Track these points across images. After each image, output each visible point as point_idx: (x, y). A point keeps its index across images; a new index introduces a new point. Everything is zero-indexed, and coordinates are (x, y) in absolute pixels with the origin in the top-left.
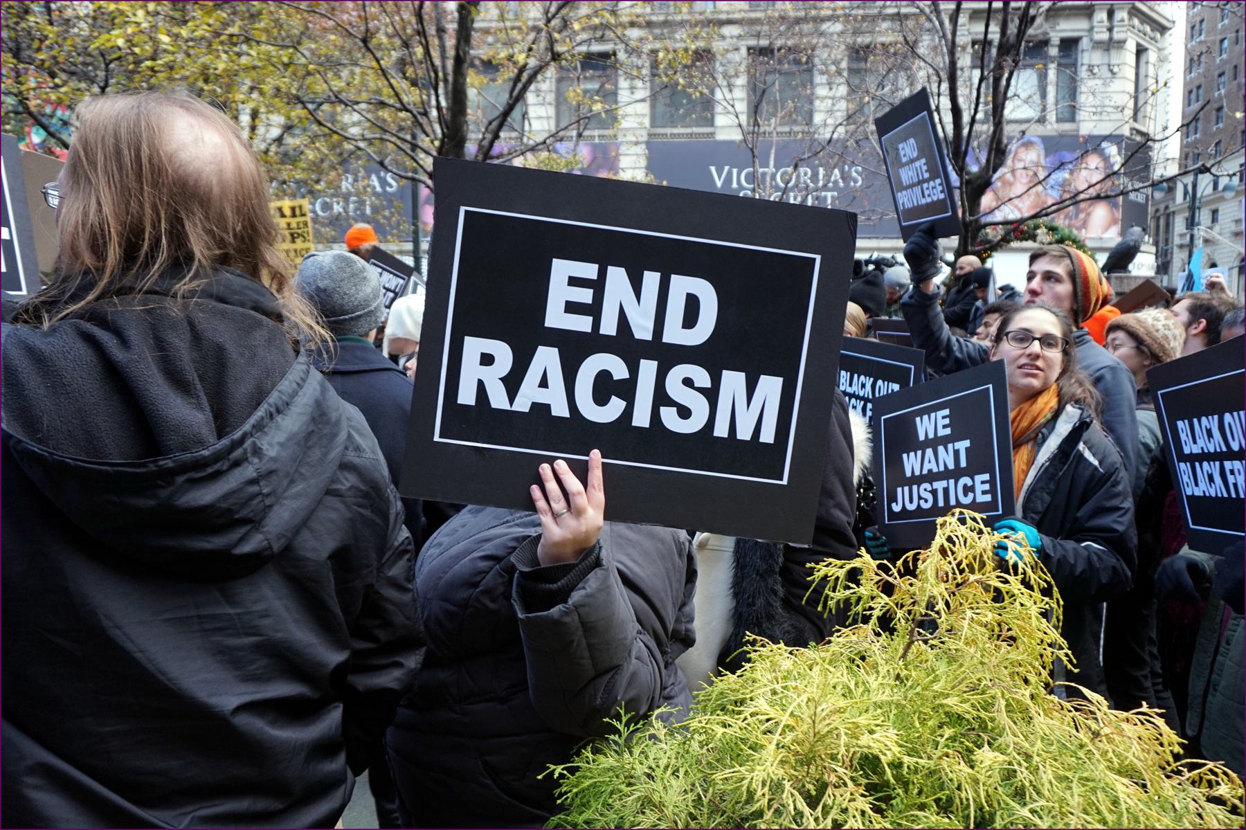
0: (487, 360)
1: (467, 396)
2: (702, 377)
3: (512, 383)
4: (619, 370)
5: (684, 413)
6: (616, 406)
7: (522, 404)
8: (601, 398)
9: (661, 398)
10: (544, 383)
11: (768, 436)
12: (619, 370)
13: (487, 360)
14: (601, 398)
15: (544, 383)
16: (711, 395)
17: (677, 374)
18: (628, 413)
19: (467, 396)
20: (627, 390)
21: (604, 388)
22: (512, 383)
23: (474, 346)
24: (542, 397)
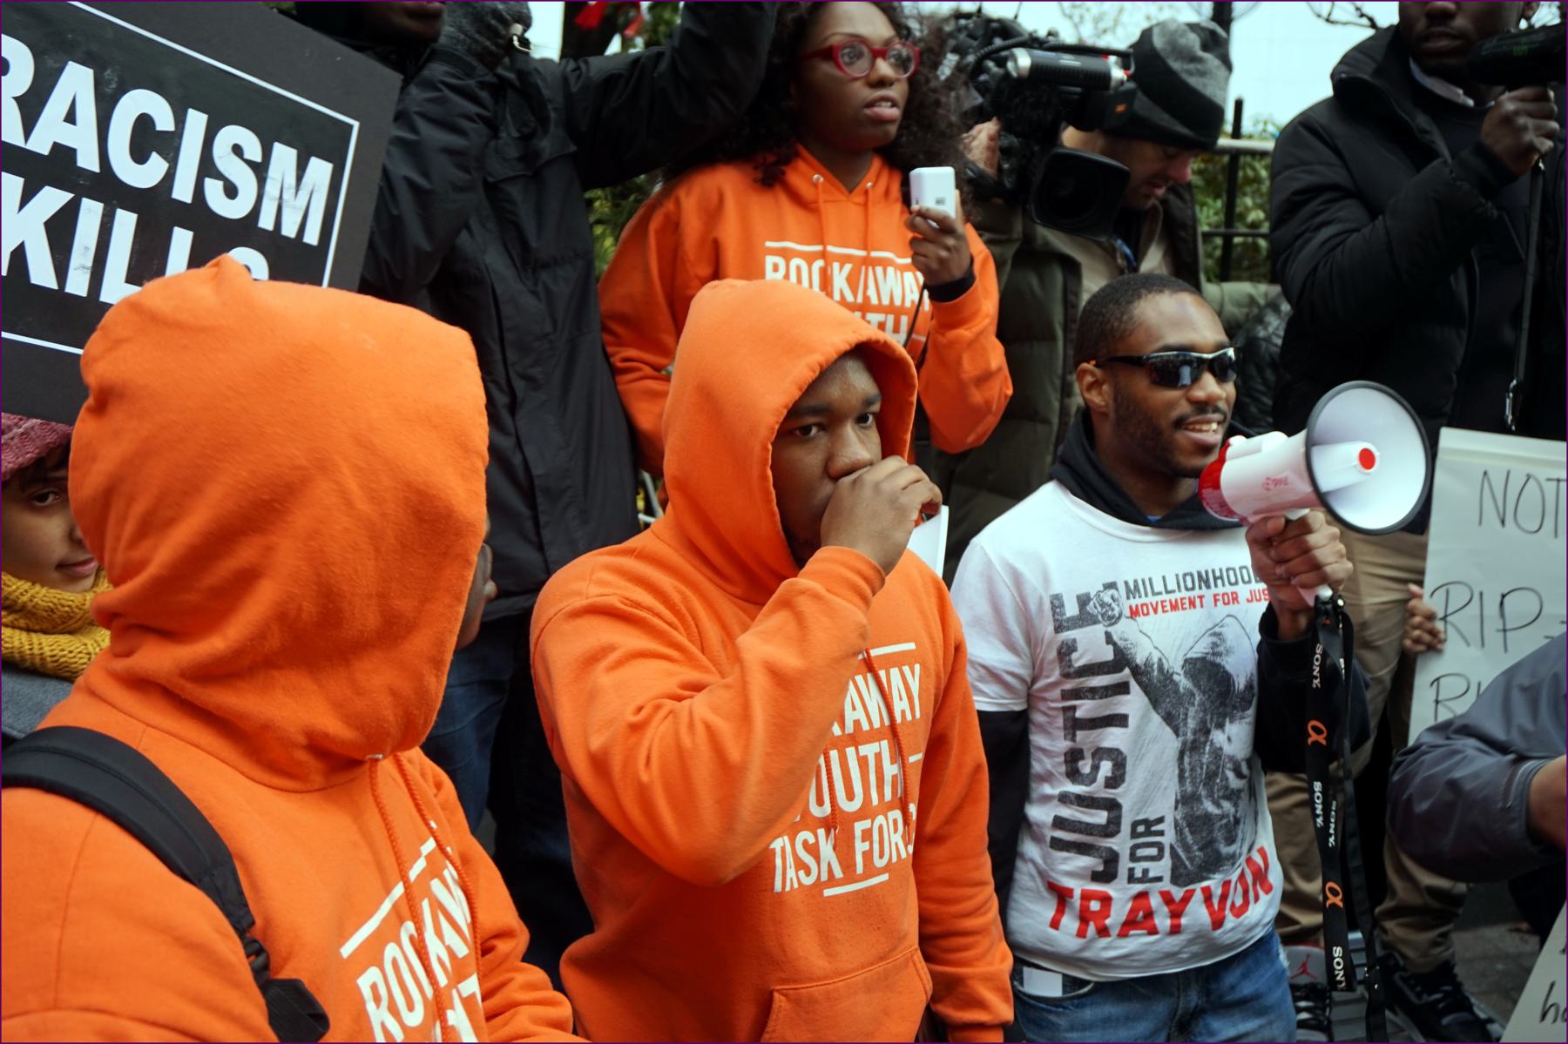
4: (164, 120)
5: (231, 191)
7: (40, 143)
8: (139, 154)
9: (207, 167)
10: (71, 118)
11: (312, 237)
14: (139, 154)
15: (71, 118)
16: (260, 170)
17: (232, 134)
18: (169, 177)
20: (169, 146)
21: (146, 139)
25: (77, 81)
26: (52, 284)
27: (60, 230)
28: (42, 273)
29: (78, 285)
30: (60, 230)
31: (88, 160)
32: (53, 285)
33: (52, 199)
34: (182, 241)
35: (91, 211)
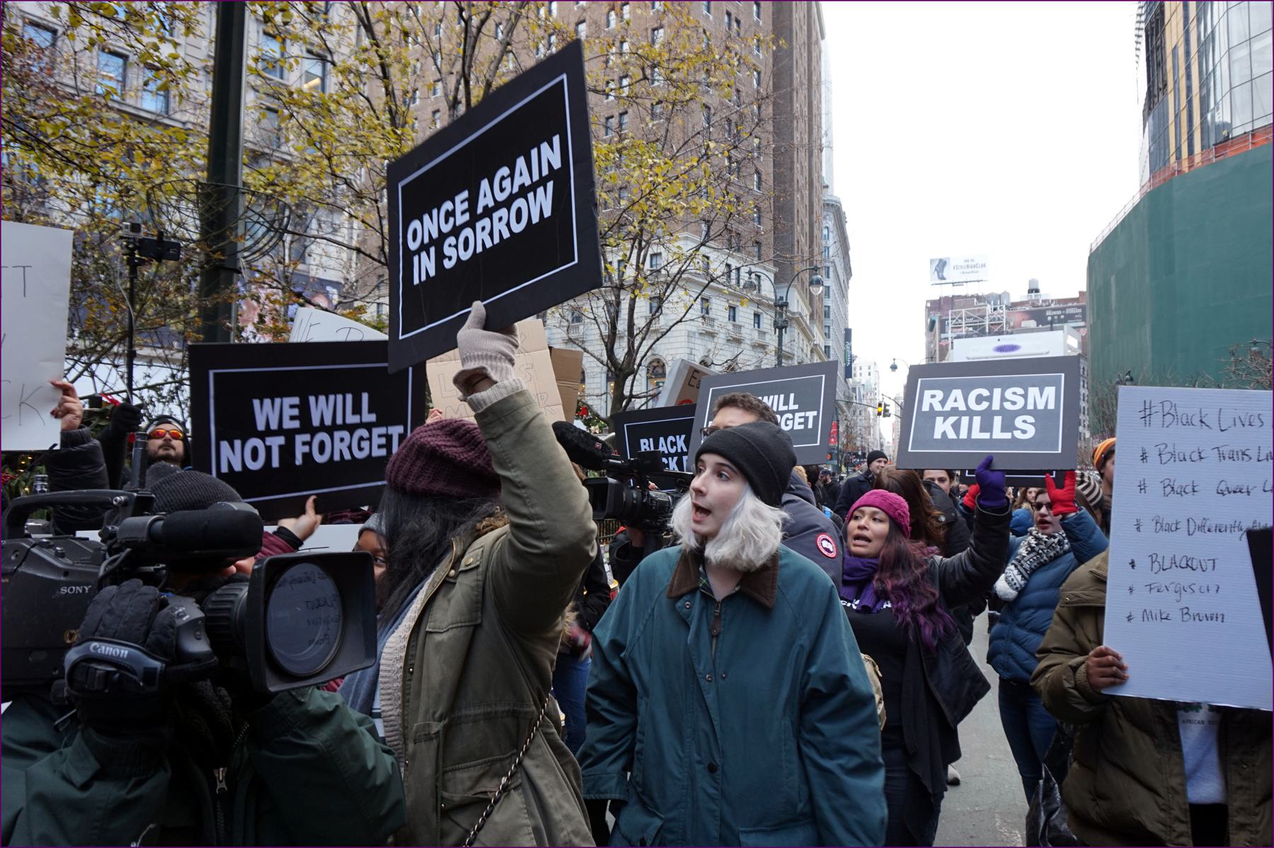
0: (933, 396)
1: (925, 408)
2: (1020, 391)
3: (943, 402)
4: (985, 393)
6: (985, 405)
7: (947, 408)
9: (1003, 399)
11: (1051, 406)
12: (985, 393)
13: (933, 396)
16: (1025, 396)
18: (990, 406)
19: (925, 408)
20: (989, 399)
21: (979, 399)
22: (943, 402)
23: (928, 393)
24: (955, 405)
25: (957, 393)
26: (954, 437)
27: (956, 427)
28: (951, 435)
29: (963, 435)
30: (956, 427)
31: (962, 408)
32: (954, 437)
33: (952, 419)
34: (998, 421)
35: (965, 420)
